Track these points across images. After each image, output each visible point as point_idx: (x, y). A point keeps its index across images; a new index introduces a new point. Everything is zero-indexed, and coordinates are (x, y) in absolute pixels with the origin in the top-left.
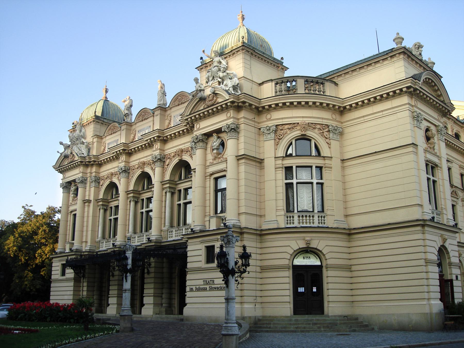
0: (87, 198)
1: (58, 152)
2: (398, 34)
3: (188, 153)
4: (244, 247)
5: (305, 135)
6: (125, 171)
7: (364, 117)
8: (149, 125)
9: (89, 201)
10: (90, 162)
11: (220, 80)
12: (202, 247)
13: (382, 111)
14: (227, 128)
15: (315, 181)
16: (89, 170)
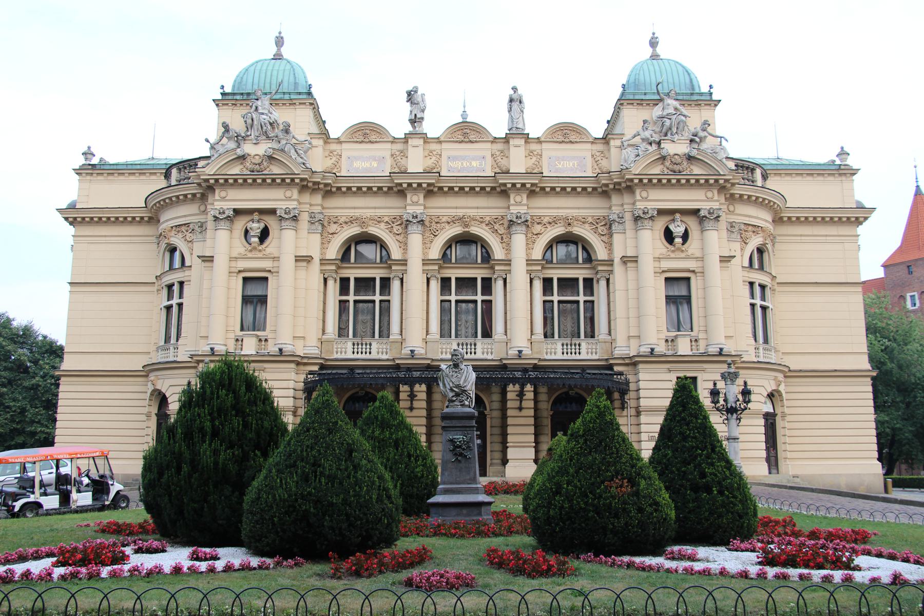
0: (303, 253)
1: (207, 141)
2: (842, 148)
3: (587, 226)
4: (745, 383)
5: (765, 244)
6: (422, 222)
7: (801, 236)
8: (481, 154)
9: (308, 259)
10: (315, 183)
11: (698, 140)
12: (673, 377)
13: (826, 236)
14: (709, 213)
15: (771, 307)
16: (306, 198)
